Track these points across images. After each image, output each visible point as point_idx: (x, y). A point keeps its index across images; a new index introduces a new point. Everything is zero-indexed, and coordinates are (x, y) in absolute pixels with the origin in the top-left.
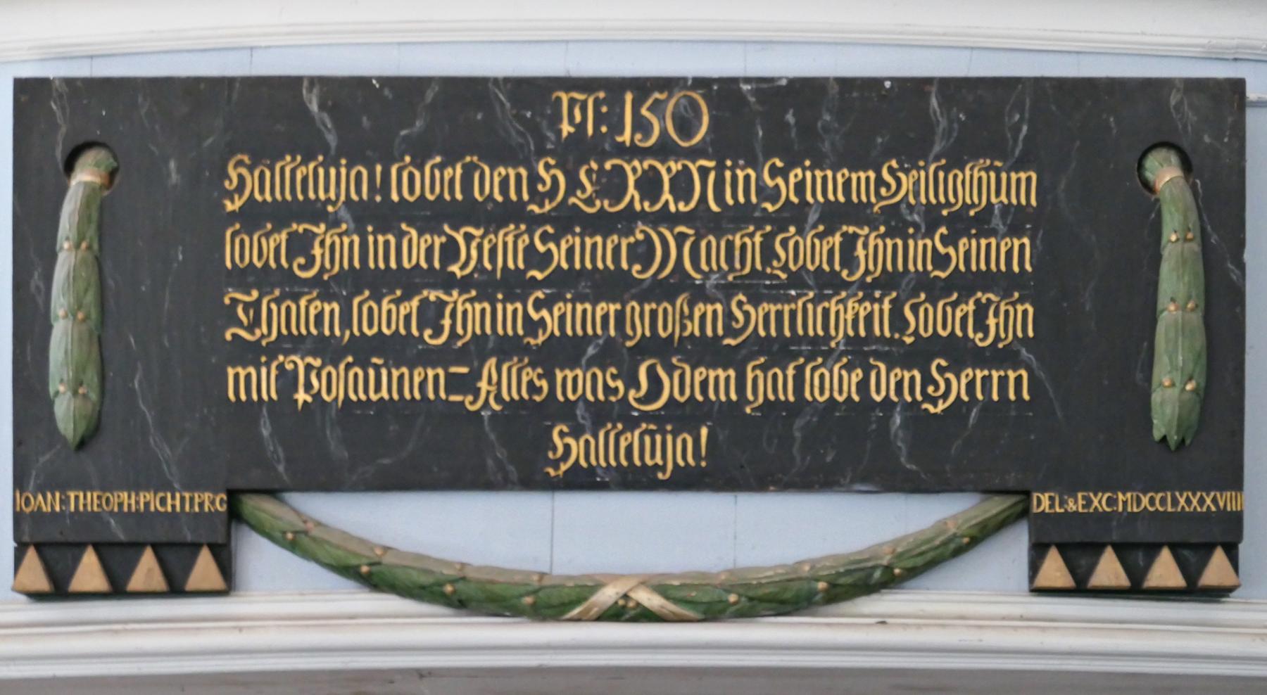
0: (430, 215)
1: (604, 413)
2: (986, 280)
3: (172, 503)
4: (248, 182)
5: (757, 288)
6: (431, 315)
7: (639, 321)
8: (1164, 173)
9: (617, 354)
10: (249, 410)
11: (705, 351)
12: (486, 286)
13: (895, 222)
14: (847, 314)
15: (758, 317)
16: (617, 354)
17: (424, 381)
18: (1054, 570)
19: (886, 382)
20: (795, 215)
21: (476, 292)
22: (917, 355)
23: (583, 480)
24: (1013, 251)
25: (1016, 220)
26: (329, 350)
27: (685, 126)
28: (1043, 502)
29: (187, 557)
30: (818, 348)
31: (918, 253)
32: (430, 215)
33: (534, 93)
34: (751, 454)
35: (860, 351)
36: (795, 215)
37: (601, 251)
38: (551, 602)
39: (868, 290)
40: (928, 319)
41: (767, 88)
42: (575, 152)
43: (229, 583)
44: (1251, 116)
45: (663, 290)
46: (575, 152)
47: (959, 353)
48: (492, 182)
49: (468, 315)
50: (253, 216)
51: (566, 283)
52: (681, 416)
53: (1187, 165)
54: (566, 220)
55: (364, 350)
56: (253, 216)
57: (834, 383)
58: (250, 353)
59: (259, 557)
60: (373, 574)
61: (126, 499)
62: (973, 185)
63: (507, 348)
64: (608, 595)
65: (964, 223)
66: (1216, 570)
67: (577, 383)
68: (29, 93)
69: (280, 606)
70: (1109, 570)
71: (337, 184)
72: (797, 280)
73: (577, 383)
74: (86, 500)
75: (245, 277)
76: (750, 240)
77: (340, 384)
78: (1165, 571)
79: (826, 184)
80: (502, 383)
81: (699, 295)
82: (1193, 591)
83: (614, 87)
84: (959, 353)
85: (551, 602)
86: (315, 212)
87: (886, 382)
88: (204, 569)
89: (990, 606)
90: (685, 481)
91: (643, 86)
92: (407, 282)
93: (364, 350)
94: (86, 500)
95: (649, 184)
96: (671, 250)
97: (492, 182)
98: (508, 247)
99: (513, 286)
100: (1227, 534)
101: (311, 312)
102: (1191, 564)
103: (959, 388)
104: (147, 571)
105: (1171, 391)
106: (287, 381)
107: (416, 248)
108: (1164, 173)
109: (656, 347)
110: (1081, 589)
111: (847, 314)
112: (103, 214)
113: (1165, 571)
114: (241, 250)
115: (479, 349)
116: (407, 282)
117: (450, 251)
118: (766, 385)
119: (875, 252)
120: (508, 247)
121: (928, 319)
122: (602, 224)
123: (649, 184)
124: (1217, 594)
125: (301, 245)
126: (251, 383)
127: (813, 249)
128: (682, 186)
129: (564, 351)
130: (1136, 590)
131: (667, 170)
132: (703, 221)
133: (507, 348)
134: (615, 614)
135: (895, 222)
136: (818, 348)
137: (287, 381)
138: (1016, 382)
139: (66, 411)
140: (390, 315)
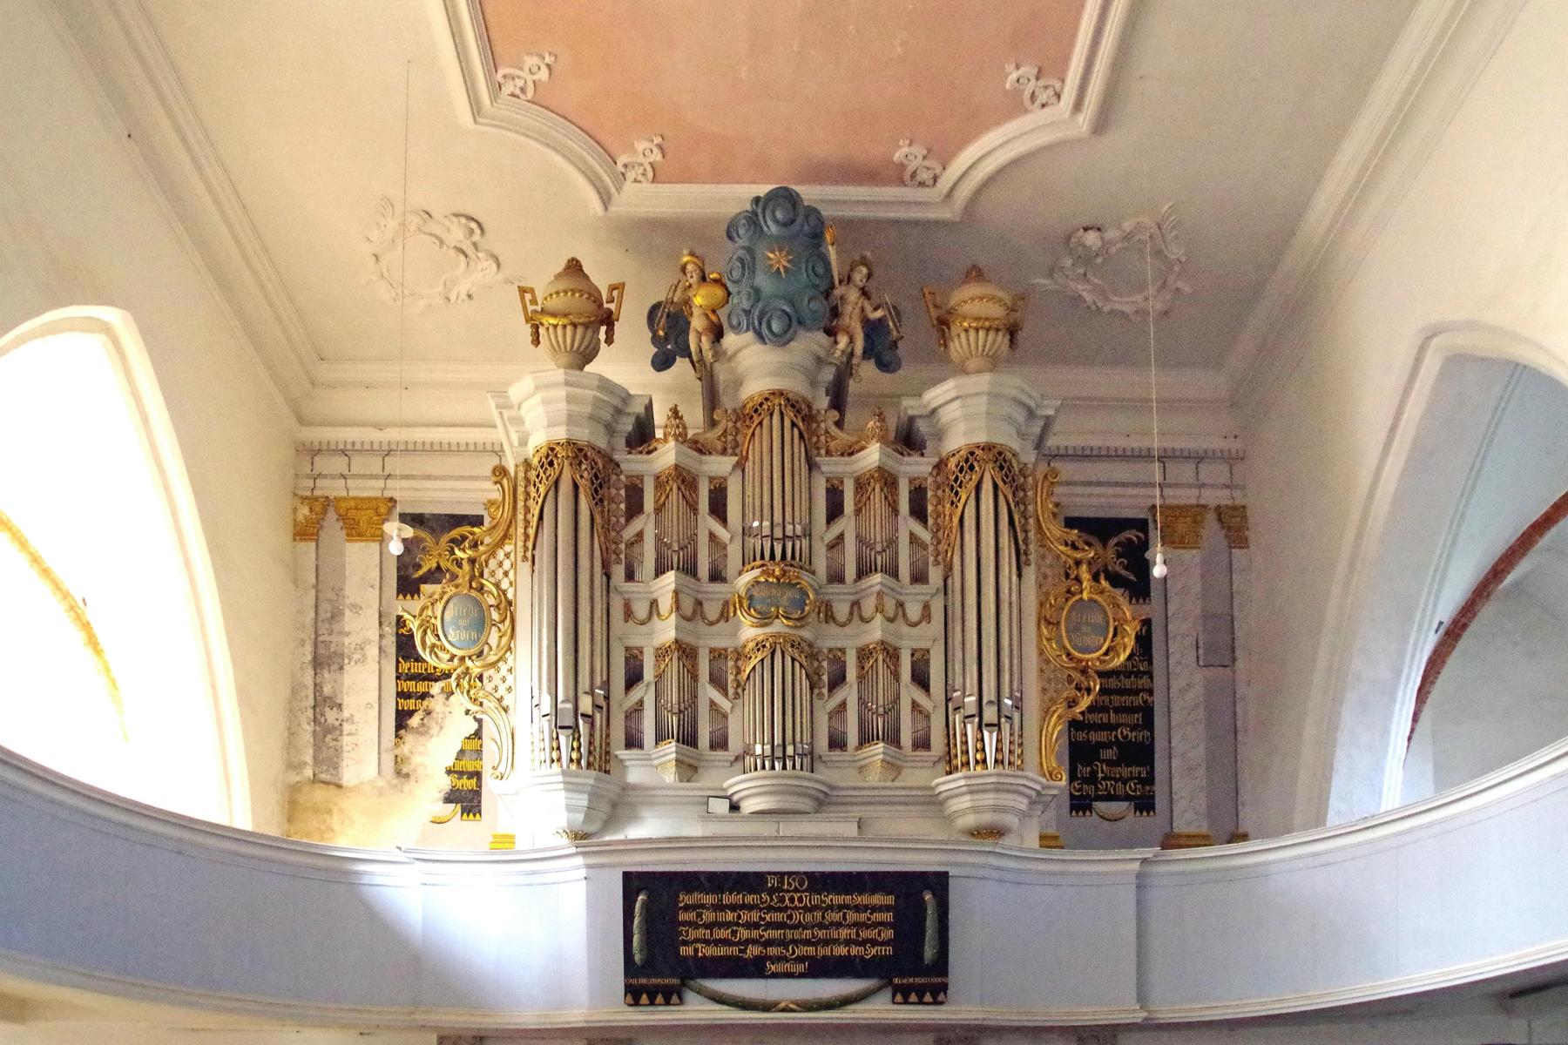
0: (733, 908)
1: (780, 959)
2: (881, 924)
3: (667, 981)
4: (686, 899)
5: (821, 926)
6: (734, 933)
7: (789, 934)
8: (928, 897)
9: (783, 943)
10: (686, 958)
11: (807, 942)
12: (750, 925)
13: (857, 909)
14: (844, 933)
15: (821, 934)
16: (783, 943)
17: (734, 950)
18: (899, 998)
19: (854, 950)
20: (831, 907)
21: (745, 928)
22: (863, 943)
23: (775, 976)
24: (888, 917)
25: (887, 908)
26: (707, 942)
27: (801, 884)
28: (896, 981)
29: (670, 995)
30: (836, 941)
31: (863, 917)
32: (733, 908)
33: (761, 877)
34: (820, 969)
35: (848, 942)
36: (831, 907)
37: (779, 917)
38: (767, 1007)
39: (849, 926)
40: (866, 934)
41: (823, 874)
42: (771, 892)
43: (681, 1002)
44: (951, 882)
45: (795, 927)
46: (771, 892)
47: (874, 943)
48: (750, 899)
49: (744, 934)
50: (687, 908)
51: (770, 925)
52: (801, 959)
53: (934, 895)
54: (770, 909)
55: (718, 942)
56: (687, 908)
57: (842, 951)
58: (685, 943)
59: (690, 996)
60: (720, 999)
61: (654, 981)
62: (877, 899)
63: (754, 942)
64: (782, 1005)
65: (874, 909)
66: (941, 997)
67: (773, 951)
68: (626, 875)
69: (695, 1010)
70: (913, 998)
71: (709, 899)
72: (832, 924)
73: (773, 951)
74: (644, 981)
75: (684, 924)
76: (819, 914)
77: (710, 951)
78: (928, 998)
79: (838, 899)
80: (753, 951)
81: (805, 928)
82: (936, 1002)
83: (781, 875)
84: (874, 943)
85: (767, 1007)
86: (703, 906)
87: (854, 950)
88: (675, 998)
89: (882, 1009)
90: (802, 976)
91: (790, 874)
92: (727, 925)
93: (718, 942)
94: (644, 981)
95: (792, 900)
96: (797, 917)
97: (750, 899)
98: (754, 916)
99: (756, 926)
100: (944, 988)
101: (701, 933)
102: (935, 997)
103: (874, 952)
104: (659, 999)
105: (929, 953)
106: (696, 951)
107: (730, 916)
108: (928, 897)
109: (794, 942)
110: (906, 1002)
111: (844, 933)
112: (647, 907)
113: (928, 998)
114: (683, 916)
115: (748, 942)
116: (727, 925)
117: (739, 917)
118: (823, 951)
119: (852, 916)
120: (754, 916)
121: (866, 934)
122: (780, 910)
123: (792, 900)
124: (941, 1003)
125: (699, 915)
126: (687, 951)
127: (835, 916)
128: (800, 900)
129: (769, 943)
130: (921, 1002)
131: (796, 896)
132: (807, 909)
133: (754, 942)
134: (783, 1010)
135: (857, 909)
136: (836, 941)
137: (696, 951)
138: (889, 950)
139: (637, 958)
140: (723, 934)
